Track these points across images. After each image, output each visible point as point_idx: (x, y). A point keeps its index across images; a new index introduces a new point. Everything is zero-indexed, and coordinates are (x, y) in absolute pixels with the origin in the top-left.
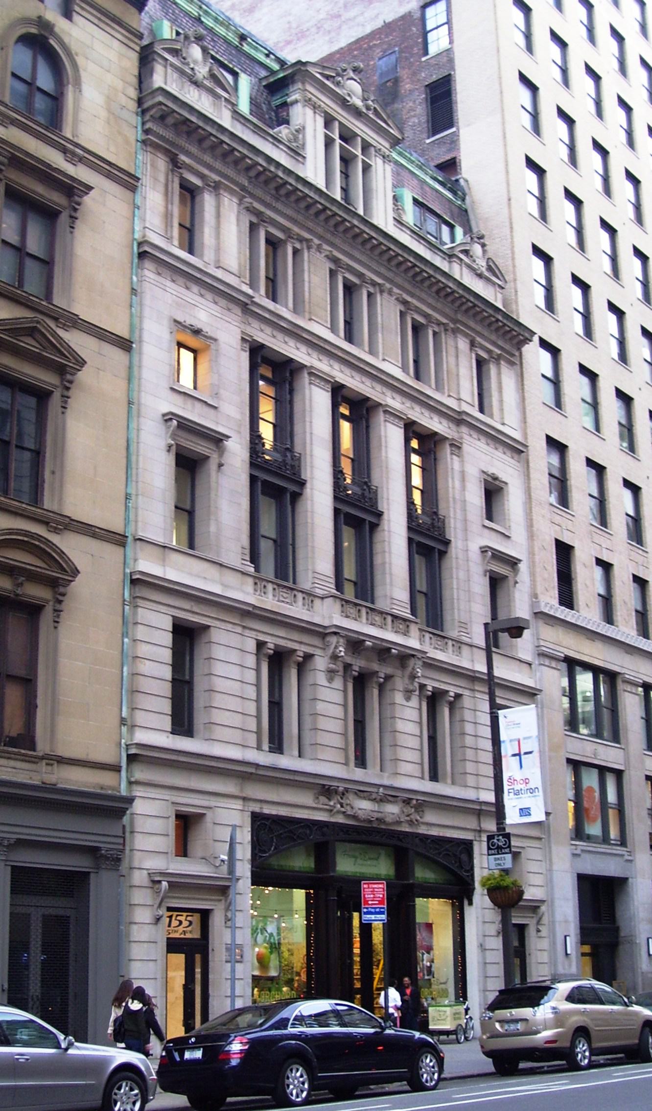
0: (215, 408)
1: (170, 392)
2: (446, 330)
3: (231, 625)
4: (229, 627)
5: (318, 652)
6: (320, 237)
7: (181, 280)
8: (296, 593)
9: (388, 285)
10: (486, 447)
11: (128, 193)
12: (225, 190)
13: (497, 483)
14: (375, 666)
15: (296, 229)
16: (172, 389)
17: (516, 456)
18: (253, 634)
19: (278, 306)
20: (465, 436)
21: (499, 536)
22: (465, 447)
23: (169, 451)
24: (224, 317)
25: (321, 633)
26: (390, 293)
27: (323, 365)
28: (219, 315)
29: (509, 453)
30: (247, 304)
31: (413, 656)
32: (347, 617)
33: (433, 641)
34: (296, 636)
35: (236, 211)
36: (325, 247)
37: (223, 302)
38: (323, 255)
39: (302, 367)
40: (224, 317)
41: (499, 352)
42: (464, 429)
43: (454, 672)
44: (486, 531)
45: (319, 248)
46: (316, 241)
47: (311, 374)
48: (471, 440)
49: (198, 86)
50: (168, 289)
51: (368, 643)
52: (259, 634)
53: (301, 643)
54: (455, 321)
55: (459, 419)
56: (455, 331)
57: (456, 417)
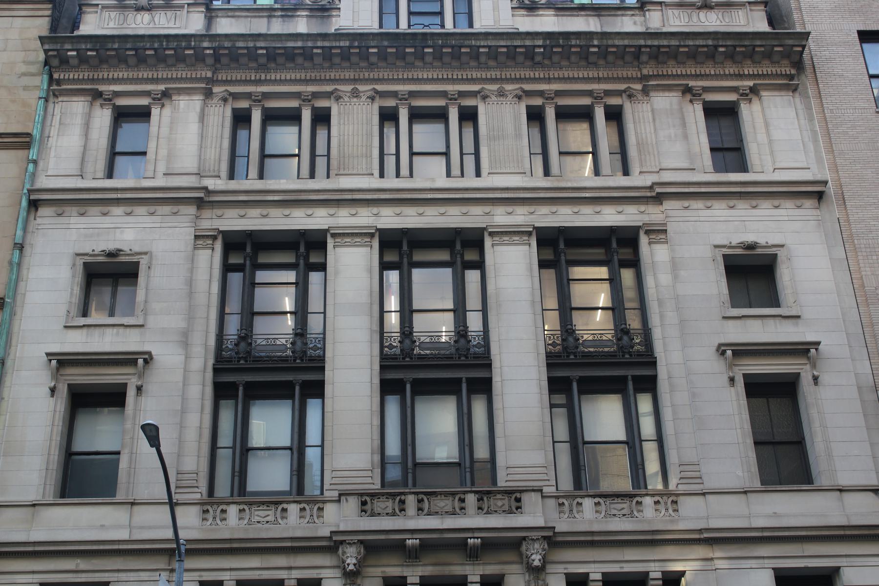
0: (142, 326)
1: (65, 331)
2: (630, 96)
3: (148, 574)
4: (144, 576)
5: (324, 573)
6: (355, 81)
7: (95, 210)
8: (285, 506)
9: (494, 87)
10: (798, 212)
11: (21, 153)
12: (179, 94)
13: (759, 251)
14: (458, 570)
15: (311, 88)
16: (66, 327)
17: (808, 203)
18: (196, 576)
19: (269, 182)
20: (670, 213)
21: (778, 320)
22: (669, 228)
23: (52, 396)
24: (163, 225)
25: (332, 545)
26: (501, 94)
27: (344, 218)
28: (158, 225)
29: (788, 204)
30: (202, 198)
31: (524, 538)
32: (373, 515)
33: (603, 508)
34: (281, 561)
35: (198, 109)
36: (361, 88)
37: (167, 209)
38: (364, 98)
39: (324, 232)
40: (163, 225)
41: (751, 83)
42: (668, 204)
43: (592, 544)
44: (731, 323)
45: (355, 94)
46: (348, 88)
47: (334, 236)
48: (695, 213)
49: (148, 10)
50: (71, 226)
51: (409, 542)
52: (203, 573)
53: (290, 568)
54: (644, 78)
55: (656, 196)
56: (646, 91)
57: (649, 194)
